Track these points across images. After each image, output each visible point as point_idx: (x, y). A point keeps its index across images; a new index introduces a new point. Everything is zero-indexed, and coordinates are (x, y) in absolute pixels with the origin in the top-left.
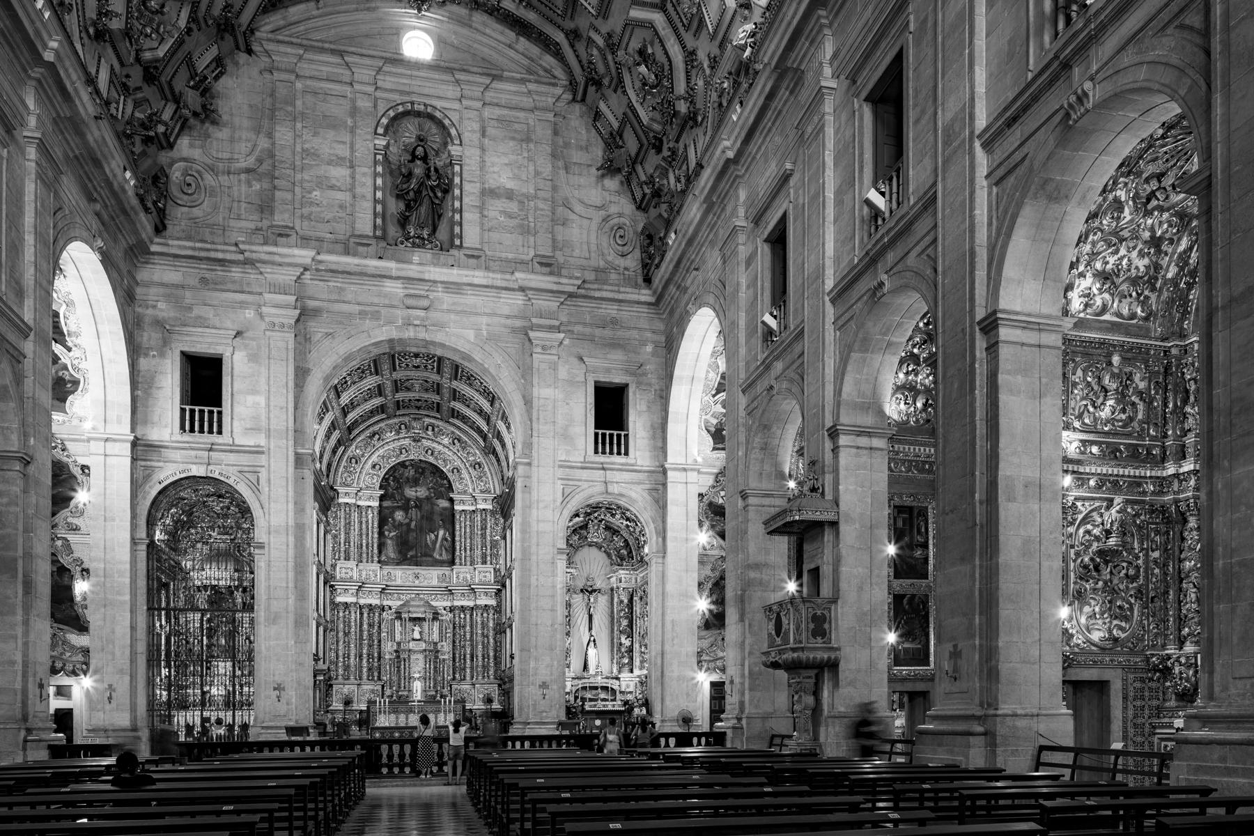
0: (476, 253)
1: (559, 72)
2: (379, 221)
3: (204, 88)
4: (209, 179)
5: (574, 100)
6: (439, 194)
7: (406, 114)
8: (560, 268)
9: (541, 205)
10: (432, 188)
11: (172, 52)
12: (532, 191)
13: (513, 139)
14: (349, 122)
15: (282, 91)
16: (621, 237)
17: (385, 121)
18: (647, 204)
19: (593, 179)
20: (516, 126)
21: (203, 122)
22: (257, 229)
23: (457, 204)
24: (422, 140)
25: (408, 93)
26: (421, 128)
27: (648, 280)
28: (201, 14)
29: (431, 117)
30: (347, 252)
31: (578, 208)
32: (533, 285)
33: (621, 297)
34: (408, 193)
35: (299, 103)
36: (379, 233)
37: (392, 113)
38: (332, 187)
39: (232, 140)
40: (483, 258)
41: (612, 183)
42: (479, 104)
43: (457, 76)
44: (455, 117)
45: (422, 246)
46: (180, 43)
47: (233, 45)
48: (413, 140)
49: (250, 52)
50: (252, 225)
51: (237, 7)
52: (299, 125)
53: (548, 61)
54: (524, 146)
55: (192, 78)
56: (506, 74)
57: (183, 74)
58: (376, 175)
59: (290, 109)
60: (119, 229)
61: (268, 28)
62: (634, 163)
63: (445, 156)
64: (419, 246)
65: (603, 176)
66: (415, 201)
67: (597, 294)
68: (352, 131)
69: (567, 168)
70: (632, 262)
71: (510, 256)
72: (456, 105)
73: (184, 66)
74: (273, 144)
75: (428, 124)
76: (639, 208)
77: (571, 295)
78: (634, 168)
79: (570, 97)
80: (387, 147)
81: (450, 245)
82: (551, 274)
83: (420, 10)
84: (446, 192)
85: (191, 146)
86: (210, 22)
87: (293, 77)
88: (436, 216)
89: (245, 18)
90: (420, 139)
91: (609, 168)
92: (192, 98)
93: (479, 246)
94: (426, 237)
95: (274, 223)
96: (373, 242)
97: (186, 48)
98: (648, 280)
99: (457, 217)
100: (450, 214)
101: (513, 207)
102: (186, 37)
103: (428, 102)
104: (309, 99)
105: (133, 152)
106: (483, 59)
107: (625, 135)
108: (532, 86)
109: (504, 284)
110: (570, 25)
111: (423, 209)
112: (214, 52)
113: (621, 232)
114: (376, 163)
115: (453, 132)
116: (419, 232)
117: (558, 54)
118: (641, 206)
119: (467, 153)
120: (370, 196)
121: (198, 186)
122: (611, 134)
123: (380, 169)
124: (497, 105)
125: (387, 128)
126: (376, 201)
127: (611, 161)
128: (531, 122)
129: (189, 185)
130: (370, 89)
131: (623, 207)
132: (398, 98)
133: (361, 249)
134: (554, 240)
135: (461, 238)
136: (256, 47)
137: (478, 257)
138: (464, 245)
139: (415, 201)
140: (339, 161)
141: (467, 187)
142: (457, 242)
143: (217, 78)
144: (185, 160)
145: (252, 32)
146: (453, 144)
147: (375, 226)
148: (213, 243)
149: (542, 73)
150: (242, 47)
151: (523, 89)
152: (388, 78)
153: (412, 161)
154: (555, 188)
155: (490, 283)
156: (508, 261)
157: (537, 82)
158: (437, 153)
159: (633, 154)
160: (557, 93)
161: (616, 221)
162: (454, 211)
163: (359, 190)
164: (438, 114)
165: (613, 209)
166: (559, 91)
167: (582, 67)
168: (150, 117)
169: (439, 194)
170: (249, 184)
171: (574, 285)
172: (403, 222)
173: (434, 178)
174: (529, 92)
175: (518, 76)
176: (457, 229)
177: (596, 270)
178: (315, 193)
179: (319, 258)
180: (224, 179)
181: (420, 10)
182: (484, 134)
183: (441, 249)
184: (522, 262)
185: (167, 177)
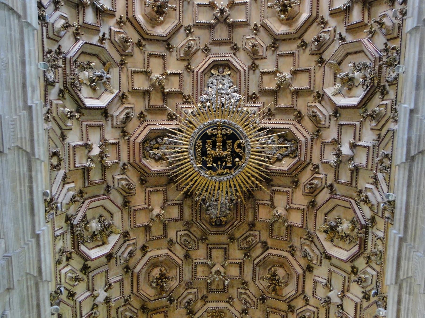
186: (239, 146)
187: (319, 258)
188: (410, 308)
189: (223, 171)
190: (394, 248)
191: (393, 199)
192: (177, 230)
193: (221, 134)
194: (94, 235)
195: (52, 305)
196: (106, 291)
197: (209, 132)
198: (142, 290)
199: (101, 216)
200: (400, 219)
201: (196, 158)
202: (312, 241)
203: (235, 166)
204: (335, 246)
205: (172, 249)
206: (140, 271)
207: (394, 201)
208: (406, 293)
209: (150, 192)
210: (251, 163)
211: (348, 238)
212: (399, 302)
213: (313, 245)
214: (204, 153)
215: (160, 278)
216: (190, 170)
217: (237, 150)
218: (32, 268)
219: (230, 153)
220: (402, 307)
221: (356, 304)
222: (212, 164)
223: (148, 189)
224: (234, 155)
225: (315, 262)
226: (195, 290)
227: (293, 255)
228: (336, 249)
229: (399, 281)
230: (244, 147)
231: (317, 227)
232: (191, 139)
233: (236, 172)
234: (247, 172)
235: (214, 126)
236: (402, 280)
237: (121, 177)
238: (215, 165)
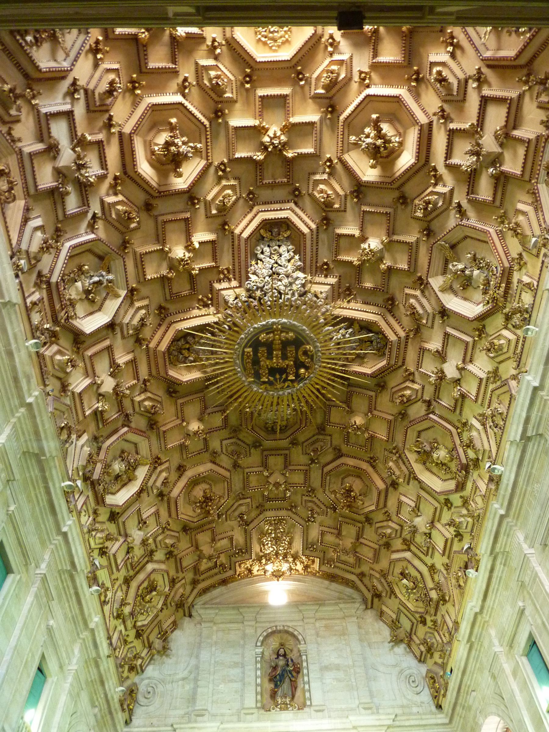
0: (321, 708)
1: (356, 595)
2: (259, 697)
3: (164, 636)
4: (160, 688)
5: (367, 608)
6: (294, 674)
7: (273, 633)
8: (378, 709)
9: (358, 670)
10: (290, 672)
11: (152, 621)
12: (351, 663)
13: (335, 635)
14: (242, 642)
15: (205, 632)
16: (413, 682)
17: (261, 638)
18: (425, 658)
19: (387, 649)
20: (336, 628)
21: (161, 656)
22: (185, 714)
23: (306, 679)
24: (282, 645)
25: (274, 621)
26: (282, 638)
27: (439, 707)
28: (169, 601)
29: (287, 632)
30: (239, 721)
31: (381, 668)
32: (362, 723)
33: (424, 722)
34: (276, 677)
35: (214, 637)
36: (259, 705)
37: (265, 634)
38: (231, 681)
39: (177, 663)
40: (326, 711)
41: (401, 649)
42: (313, 620)
43: (300, 608)
44: (300, 629)
45: (287, 709)
46: (157, 616)
47: (182, 614)
48: (277, 646)
49: (190, 616)
50: (182, 712)
51: (187, 595)
52: (214, 649)
53: (349, 591)
54: (342, 638)
55: (160, 633)
56: (327, 602)
57: (156, 631)
58: (257, 669)
59: (209, 641)
60: (105, 725)
61: (202, 602)
62: (410, 635)
63: (295, 651)
64: (284, 710)
65: (393, 646)
66: (281, 681)
67: (407, 723)
68: (243, 647)
69: (369, 645)
70: (426, 696)
71: (344, 706)
72: (301, 623)
73: (157, 627)
74: (199, 662)
75: (286, 636)
76: (420, 661)
77: (389, 727)
78: (411, 638)
79: (364, 607)
80: (263, 653)
81: (302, 706)
82: (373, 713)
83: (278, 580)
84: (298, 672)
85: (154, 670)
86: (173, 604)
87: (211, 624)
88: (294, 687)
89: (190, 600)
90: (282, 645)
91: (396, 641)
92: (158, 644)
93: (323, 704)
94: (288, 702)
95: (197, 708)
96: (255, 711)
97: (159, 618)
98: (439, 707)
99: (307, 687)
100: (302, 686)
101: (341, 675)
102: (160, 613)
103: (285, 624)
104: (220, 634)
105: (122, 677)
106: (313, 597)
107: (401, 621)
108: (341, 606)
109: (342, 726)
110: (358, 571)
111: (286, 686)
112: (172, 619)
113: (412, 679)
114: (256, 662)
115: (300, 637)
116: (284, 700)
117: (354, 587)
118: (421, 660)
119: (309, 648)
120: (253, 683)
121: (154, 693)
122: (393, 621)
123: (259, 666)
124: (324, 619)
125: (262, 642)
126: (257, 685)
127: (396, 636)
128: (344, 624)
129: (149, 693)
130: (253, 623)
131: (410, 662)
132: (268, 625)
133: (248, 717)
134: (370, 692)
135: (310, 699)
136: (194, 614)
137: (322, 711)
138: (313, 704)
139: (281, 681)
140: (236, 665)
141: (311, 667)
142: (308, 703)
143: (172, 632)
144: (149, 678)
145: (193, 606)
146: (300, 644)
147: (257, 701)
148: (158, 726)
149: (346, 598)
150: (187, 615)
151: (337, 608)
152: (262, 616)
153: (277, 658)
154: (365, 659)
155: (333, 727)
156: (342, 710)
157: (344, 603)
158: (291, 651)
159: (409, 630)
160: (358, 605)
161: (408, 672)
162: (304, 683)
163: (247, 680)
164: (291, 630)
165: (404, 665)
166: (357, 605)
167: (369, 590)
168: (135, 657)
169: (294, 674)
170: (183, 686)
171: (389, 719)
172: (273, 695)
173: (291, 665)
174: (341, 609)
175: (334, 602)
176: (307, 695)
177: (402, 707)
178: (221, 686)
179: (222, 726)
180: (169, 687)
181: (278, 580)
182: (317, 635)
183: (299, 709)
184: (352, 710)
185: (138, 689)
186: (305, 353)
187: (407, 476)
188: (504, 577)
189: (282, 384)
190: (493, 522)
191: (500, 473)
192: (221, 438)
193: (280, 339)
194: (117, 477)
195: (90, 587)
196: (140, 529)
197: (263, 337)
198: (182, 513)
199: (123, 452)
200: (504, 496)
201: (245, 369)
202: (400, 457)
203: (299, 378)
204: (428, 469)
205: (217, 461)
206: (179, 496)
207: (500, 476)
208: (501, 564)
209: (182, 404)
210: (321, 373)
211: (444, 467)
212: (492, 571)
213: (400, 461)
214: (256, 362)
215: (204, 502)
216: (238, 384)
217: (303, 358)
218: (64, 564)
219: (292, 363)
220: (495, 574)
221: (446, 541)
222: (268, 378)
223: (180, 401)
224: (299, 365)
225: (401, 480)
226: (248, 500)
227: (374, 467)
228: (428, 474)
229: (494, 553)
230: (312, 356)
231: (407, 446)
232: (236, 347)
233: (301, 385)
234: (317, 384)
235: (268, 329)
236: (498, 553)
237: (143, 397)
238: (271, 378)
